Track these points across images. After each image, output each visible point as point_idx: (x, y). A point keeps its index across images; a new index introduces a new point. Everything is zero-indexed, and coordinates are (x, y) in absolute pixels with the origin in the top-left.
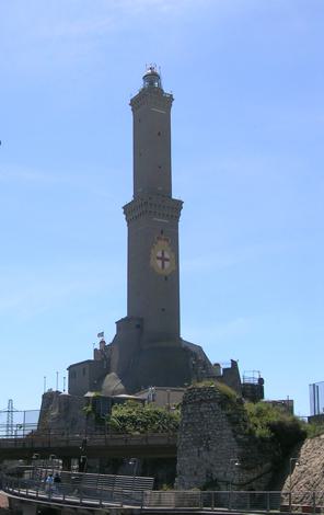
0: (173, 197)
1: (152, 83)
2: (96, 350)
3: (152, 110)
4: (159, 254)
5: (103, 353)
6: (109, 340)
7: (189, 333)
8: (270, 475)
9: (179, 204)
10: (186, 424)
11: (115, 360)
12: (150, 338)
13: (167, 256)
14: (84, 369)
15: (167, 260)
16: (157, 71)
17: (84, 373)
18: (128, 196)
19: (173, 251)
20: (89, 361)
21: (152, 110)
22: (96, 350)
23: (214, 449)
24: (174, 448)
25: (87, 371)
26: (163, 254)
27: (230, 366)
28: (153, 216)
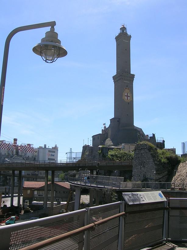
0: (131, 73)
1: (123, 31)
2: (102, 130)
3: (123, 41)
4: (126, 94)
5: (105, 131)
6: (107, 126)
7: (137, 123)
8: (167, 176)
9: (133, 76)
10: (136, 157)
11: (110, 134)
12: (123, 125)
13: (129, 95)
14: (98, 137)
15: (129, 96)
16: (125, 26)
17: (98, 139)
18: (115, 73)
19: (131, 94)
20: (100, 134)
21: (123, 41)
22: (102, 130)
23: (146, 166)
24: (131, 166)
25: (99, 138)
27: (152, 136)
28: (124, 80)
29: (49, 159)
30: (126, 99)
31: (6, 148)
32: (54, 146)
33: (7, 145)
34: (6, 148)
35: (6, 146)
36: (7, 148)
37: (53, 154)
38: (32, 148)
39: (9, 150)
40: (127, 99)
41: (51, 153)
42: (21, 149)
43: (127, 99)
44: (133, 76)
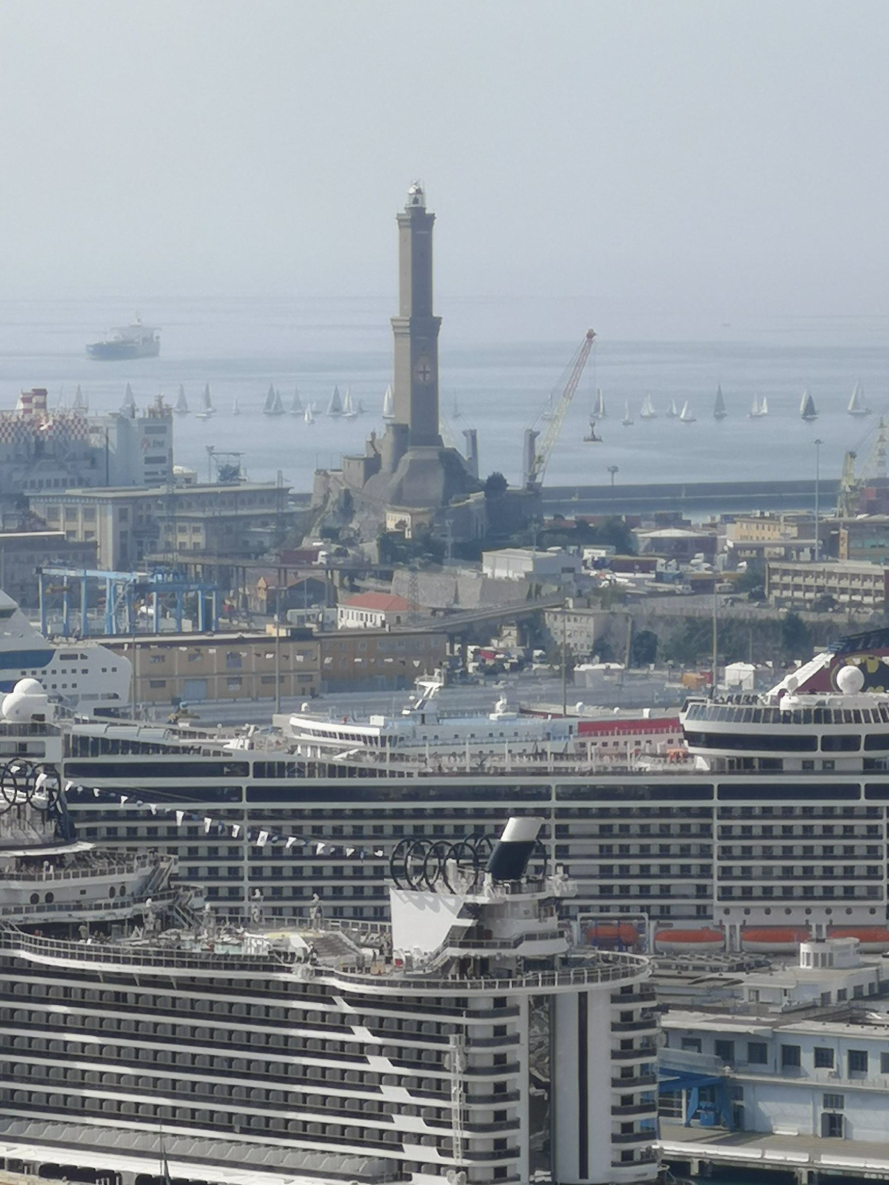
9: (438, 321)
13: (428, 369)
15: (428, 372)
26: (424, 368)
29: (148, 460)
30: (422, 379)
31: (10, 435)
32: (153, 404)
33: (13, 425)
34: (10, 435)
35: (9, 430)
36: (13, 434)
37: (160, 437)
38: (82, 422)
39: (19, 440)
40: (424, 378)
41: (152, 437)
42: (51, 433)
43: (424, 378)
44: (438, 321)
